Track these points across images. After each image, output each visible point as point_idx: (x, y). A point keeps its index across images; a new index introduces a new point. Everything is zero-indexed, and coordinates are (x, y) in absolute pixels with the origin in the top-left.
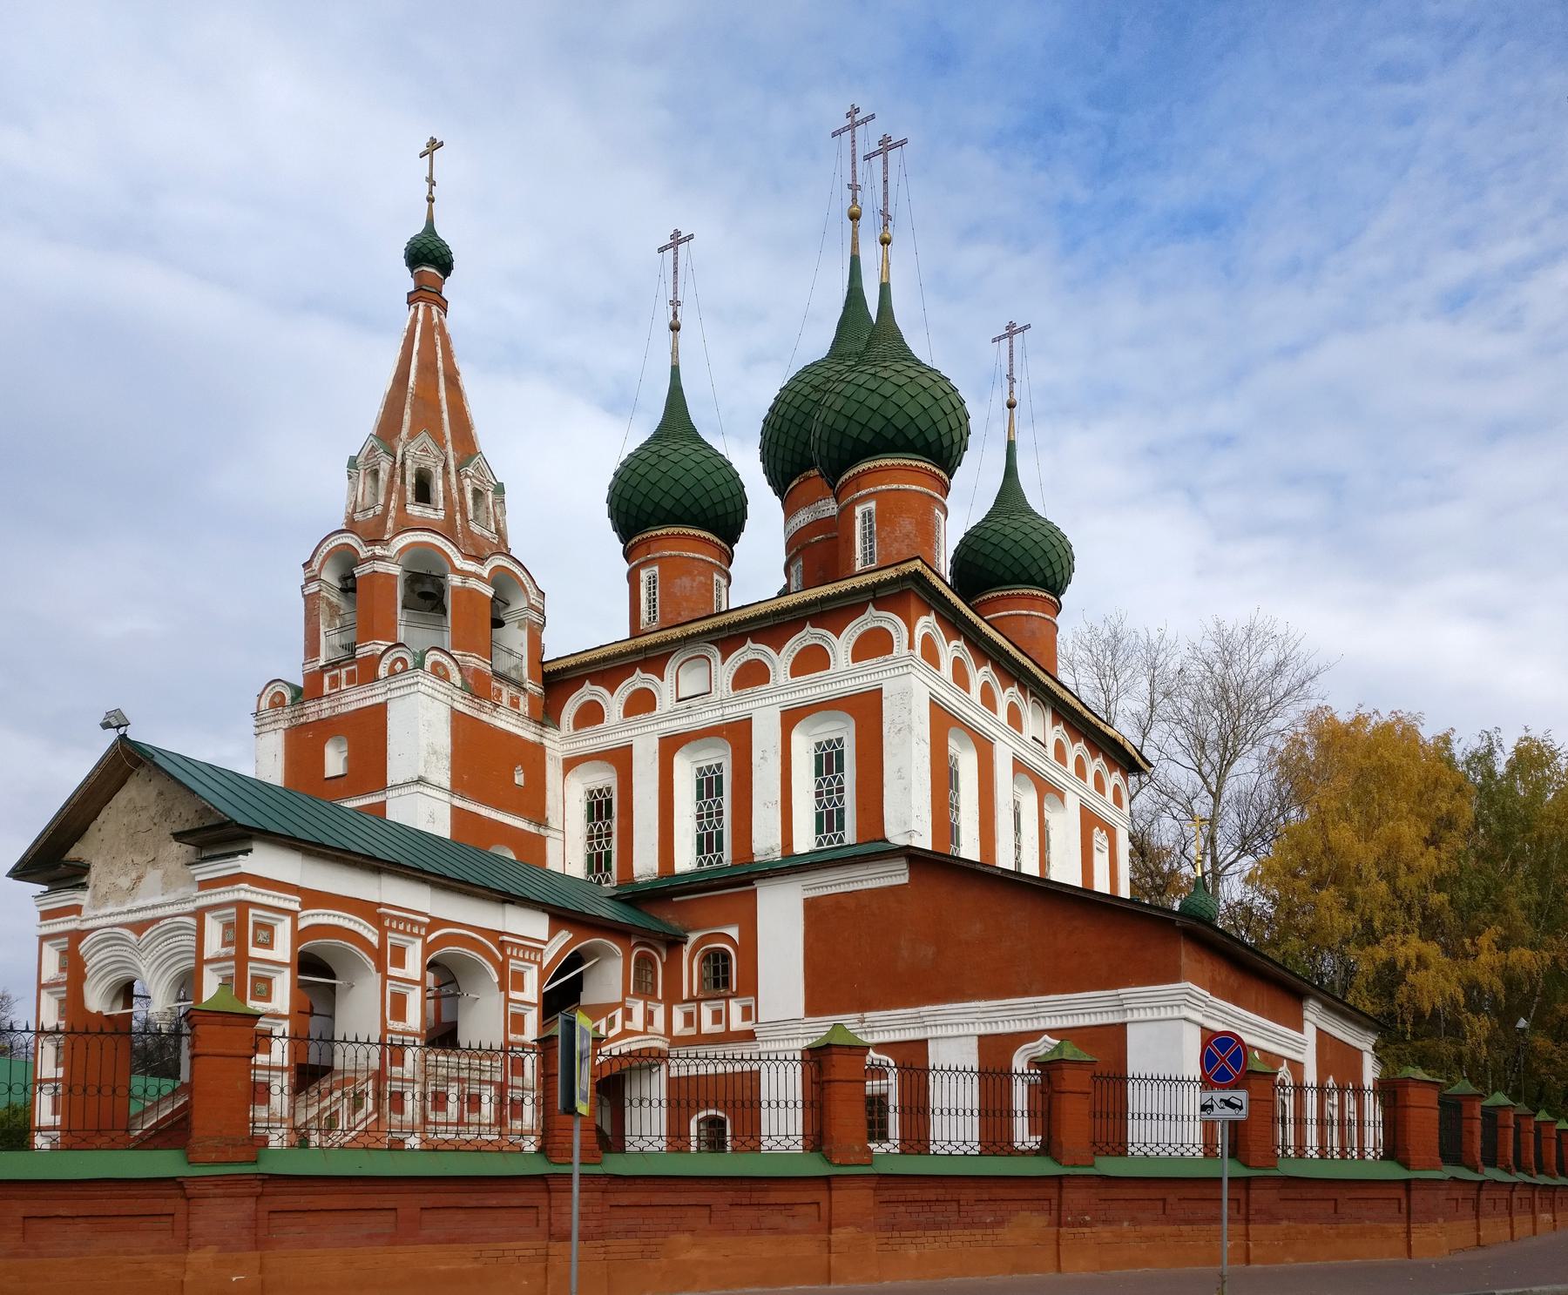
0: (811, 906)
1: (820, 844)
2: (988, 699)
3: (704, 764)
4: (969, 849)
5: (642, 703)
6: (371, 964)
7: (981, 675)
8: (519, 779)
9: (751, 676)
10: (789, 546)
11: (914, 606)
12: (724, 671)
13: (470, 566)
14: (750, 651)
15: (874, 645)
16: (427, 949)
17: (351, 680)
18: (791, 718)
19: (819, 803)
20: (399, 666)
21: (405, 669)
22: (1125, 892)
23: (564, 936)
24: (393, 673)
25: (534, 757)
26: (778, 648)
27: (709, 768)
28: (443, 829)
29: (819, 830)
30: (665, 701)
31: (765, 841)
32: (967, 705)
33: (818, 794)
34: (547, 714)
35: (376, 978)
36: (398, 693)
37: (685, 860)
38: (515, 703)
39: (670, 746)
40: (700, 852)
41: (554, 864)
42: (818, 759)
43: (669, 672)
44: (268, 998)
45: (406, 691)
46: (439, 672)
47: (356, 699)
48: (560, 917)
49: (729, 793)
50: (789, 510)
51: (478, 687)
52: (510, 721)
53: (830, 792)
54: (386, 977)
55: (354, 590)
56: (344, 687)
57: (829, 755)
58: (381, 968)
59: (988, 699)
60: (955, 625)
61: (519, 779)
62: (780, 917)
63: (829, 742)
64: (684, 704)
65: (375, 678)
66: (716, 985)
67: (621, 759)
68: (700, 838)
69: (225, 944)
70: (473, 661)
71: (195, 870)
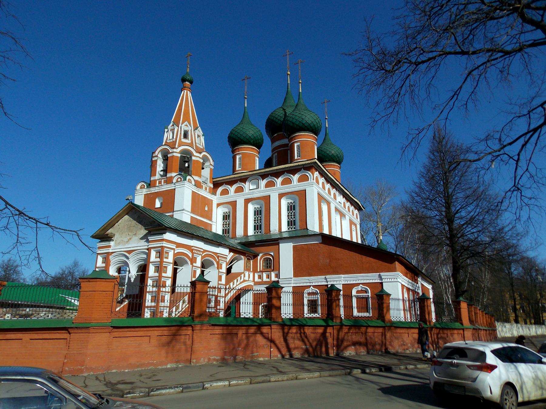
1: (289, 229)
2: (329, 193)
4: (326, 231)
5: (240, 190)
6: (189, 262)
7: (328, 186)
8: (206, 209)
9: (270, 185)
10: (273, 151)
11: (314, 170)
13: (198, 155)
15: (304, 179)
16: (202, 258)
18: (281, 196)
19: (288, 218)
20: (179, 180)
21: (181, 181)
22: (360, 242)
23: (232, 254)
24: (177, 181)
25: (209, 203)
28: (189, 221)
29: (288, 225)
30: (246, 190)
31: (274, 228)
32: (325, 194)
33: (288, 216)
34: (213, 191)
35: (191, 266)
37: (251, 231)
38: (206, 189)
39: (247, 201)
40: (255, 230)
41: (214, 230)
42: (288, 207)
44: (166, 273)
46: (190, 181)
47: (166, 187)
48: (231, 250)
49: (263, 215)
50: (273, 141)
51: (198, 185)
52: (204, 193)
53: (291, 216)
54: (193, 266)
55: (167, 160)
57: (291, 206)
58: (192, 264)
59: (329, 193)
60: (323, 174)
61: (206, 209)
62: (286, 251)
64: (251, 191)
66: (267, 268)
67: (234, 204)
68: (255, 226)
69: (156, 258)
70: (196, 178)
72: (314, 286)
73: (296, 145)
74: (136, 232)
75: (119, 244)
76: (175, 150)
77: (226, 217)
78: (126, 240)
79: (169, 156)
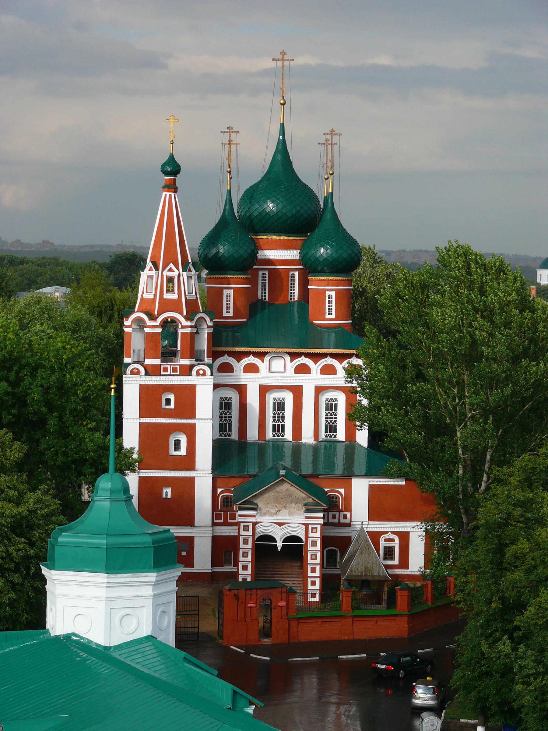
0: (371, 487)
3: (277, 397)
5: (252, 369)
9: (302, 369)
12: (291, 365)
14: (303, 360)
17: (175, 370)
18: (319, 390)
20: (201, 372)
26: (316, 363)
27: (279, 399)
36: (200, 383)
39: (264, 390)
43: (267, 358)
45: (205, 383)
56: (172, 373)
63: (332, 399)
65: (191, 375)
67: (241, 390)
71: (305, 514)
72: (393, 533)
73: (328, 293)
74: (286, 504)
75: (265, 514)
76: (189, 323)
77: (224, 405)
78: (274, 511)
79: (180, 331)
